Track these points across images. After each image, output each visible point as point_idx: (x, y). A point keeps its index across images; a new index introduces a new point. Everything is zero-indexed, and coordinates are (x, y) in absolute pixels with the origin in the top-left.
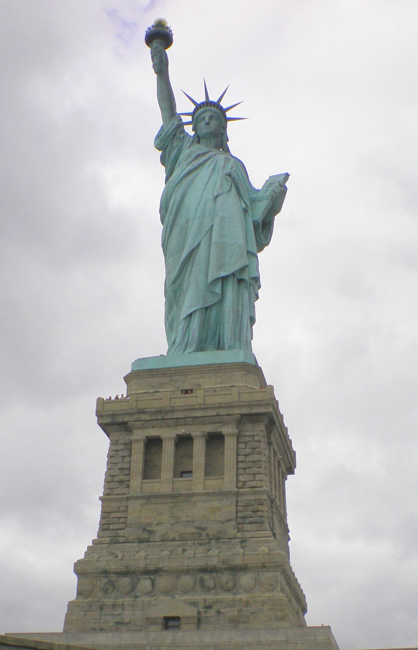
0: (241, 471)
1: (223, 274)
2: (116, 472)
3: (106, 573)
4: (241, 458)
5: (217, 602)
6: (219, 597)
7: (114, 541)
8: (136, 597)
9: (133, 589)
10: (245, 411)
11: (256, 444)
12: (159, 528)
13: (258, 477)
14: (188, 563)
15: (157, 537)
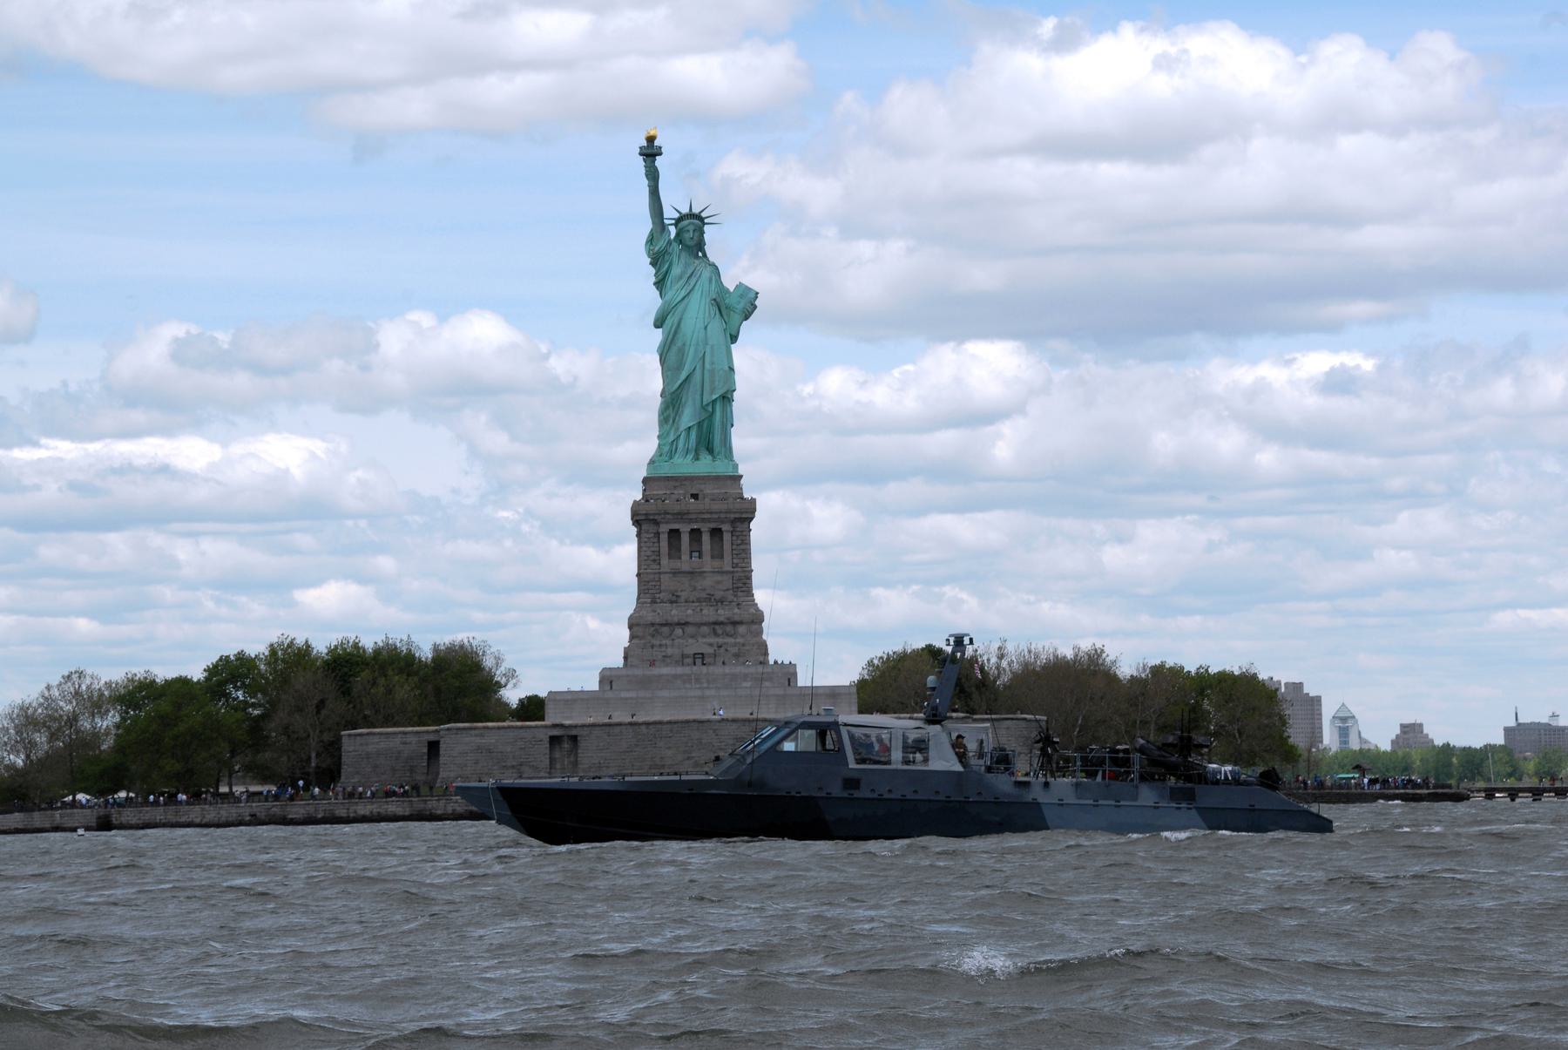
0: (735, 556)
1: (714, 397)
2: (649, 553)
3: (653, 624)
4: (734, 547)
5: (725, 643)
6: (725, 641)
7: (654, 602)
8: (673, 640)
9: (671, 635)
10: (737, 516)
11: (744, 538)
12: (683, 594)
13: (746, 560)
14: (705, 619)
15: (682, 599)
